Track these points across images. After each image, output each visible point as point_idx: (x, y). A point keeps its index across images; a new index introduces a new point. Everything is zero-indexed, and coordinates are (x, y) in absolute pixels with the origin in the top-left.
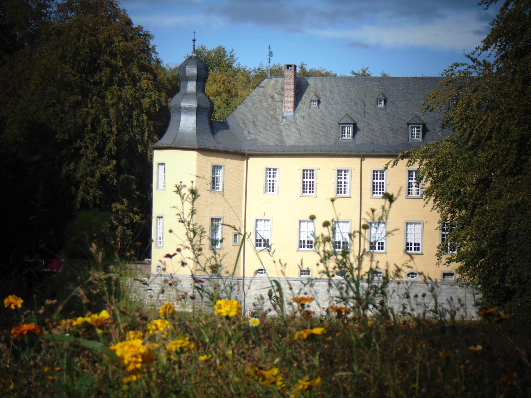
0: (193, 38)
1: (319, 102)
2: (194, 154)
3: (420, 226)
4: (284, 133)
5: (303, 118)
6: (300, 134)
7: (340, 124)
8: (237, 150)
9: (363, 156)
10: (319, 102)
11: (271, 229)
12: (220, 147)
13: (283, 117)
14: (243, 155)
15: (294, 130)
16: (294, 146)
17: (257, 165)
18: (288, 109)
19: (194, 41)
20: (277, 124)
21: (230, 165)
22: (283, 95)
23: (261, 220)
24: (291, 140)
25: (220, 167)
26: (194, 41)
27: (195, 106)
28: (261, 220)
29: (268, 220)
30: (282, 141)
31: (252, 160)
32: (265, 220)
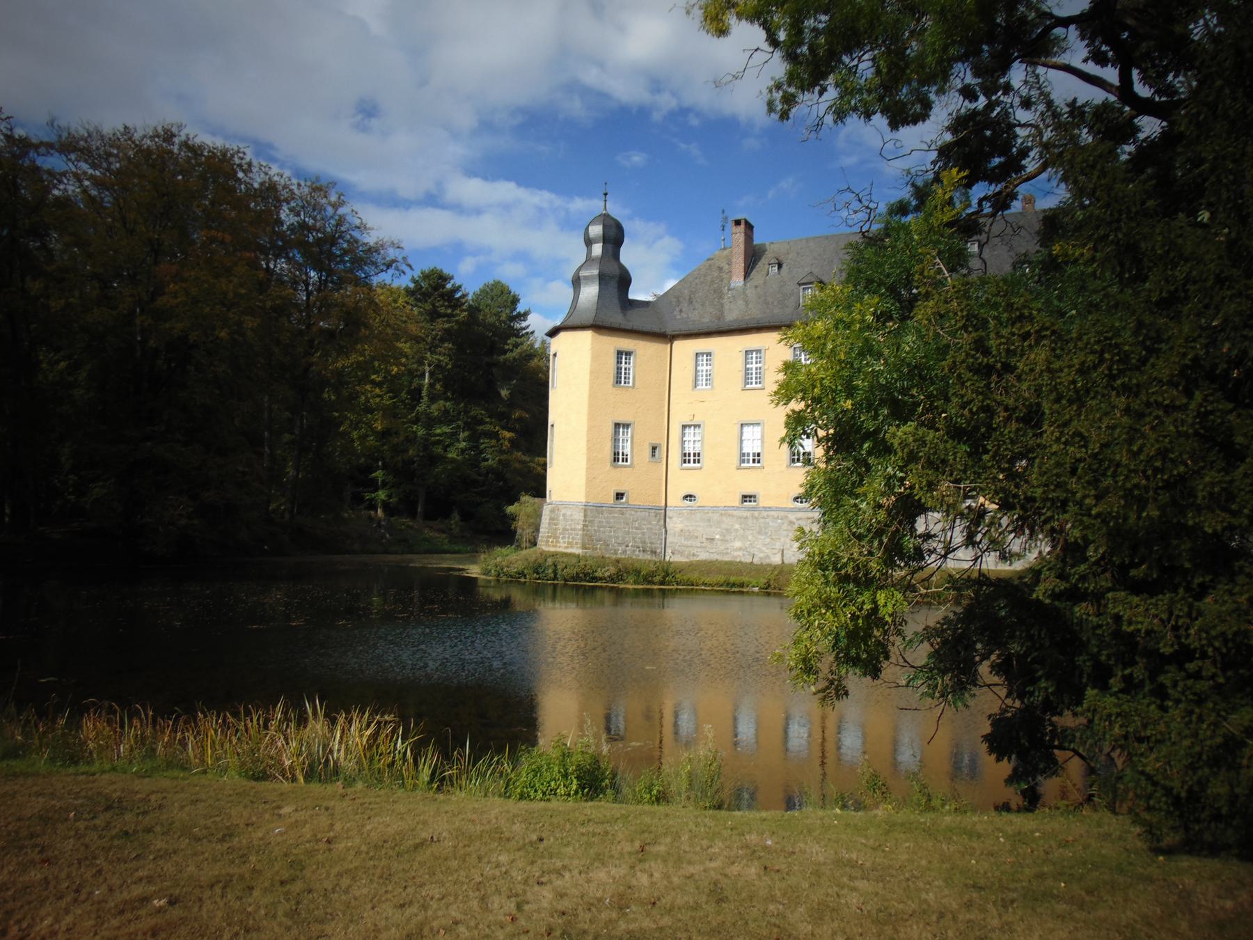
1: (780, 266)
2: (588, 335)
4: (726, 307)
7: (800, 285)
8: (656, 329)
10: (780, 266)
11: (703, 437)
12: (629, 326)
14: (667, 337)
15: (740, 302)
17: (685, 349)
18: (738, 281)
20: (721, 297)
21: (645, 350)
23: (690, 426)
24: (733, 314)
25: (629, 354)
27: (596, 272)
28: (690, 426)
30: (720, 317)
31: (678, 344)
32: (695, 426)
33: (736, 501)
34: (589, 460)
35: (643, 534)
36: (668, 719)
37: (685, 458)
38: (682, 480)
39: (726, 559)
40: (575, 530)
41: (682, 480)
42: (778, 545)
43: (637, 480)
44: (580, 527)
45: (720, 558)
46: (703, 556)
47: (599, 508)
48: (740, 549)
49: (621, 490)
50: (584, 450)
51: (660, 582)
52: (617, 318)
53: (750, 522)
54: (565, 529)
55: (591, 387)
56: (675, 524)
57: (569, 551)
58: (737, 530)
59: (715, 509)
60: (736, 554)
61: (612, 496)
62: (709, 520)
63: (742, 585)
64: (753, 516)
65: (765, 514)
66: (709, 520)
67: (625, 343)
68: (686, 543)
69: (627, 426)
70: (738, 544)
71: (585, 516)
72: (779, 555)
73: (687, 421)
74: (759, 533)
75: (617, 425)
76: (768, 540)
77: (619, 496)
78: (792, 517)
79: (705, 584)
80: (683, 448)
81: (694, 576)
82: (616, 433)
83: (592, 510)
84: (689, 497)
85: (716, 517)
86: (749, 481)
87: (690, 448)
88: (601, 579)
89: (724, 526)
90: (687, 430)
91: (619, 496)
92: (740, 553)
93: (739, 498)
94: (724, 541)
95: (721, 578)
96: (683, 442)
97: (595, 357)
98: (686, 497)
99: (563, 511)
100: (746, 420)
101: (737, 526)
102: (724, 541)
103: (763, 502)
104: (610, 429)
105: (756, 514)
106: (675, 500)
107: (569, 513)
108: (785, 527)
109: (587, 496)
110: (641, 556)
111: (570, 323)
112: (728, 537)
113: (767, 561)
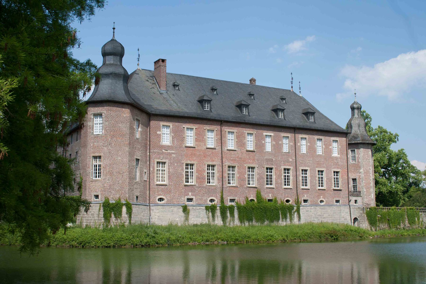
0: (113, 27)
5: (173, 95)
6: (177, 104)
19: (114, 29)
22: (154, 81)
26: (114, 29)
62: (172, 211)
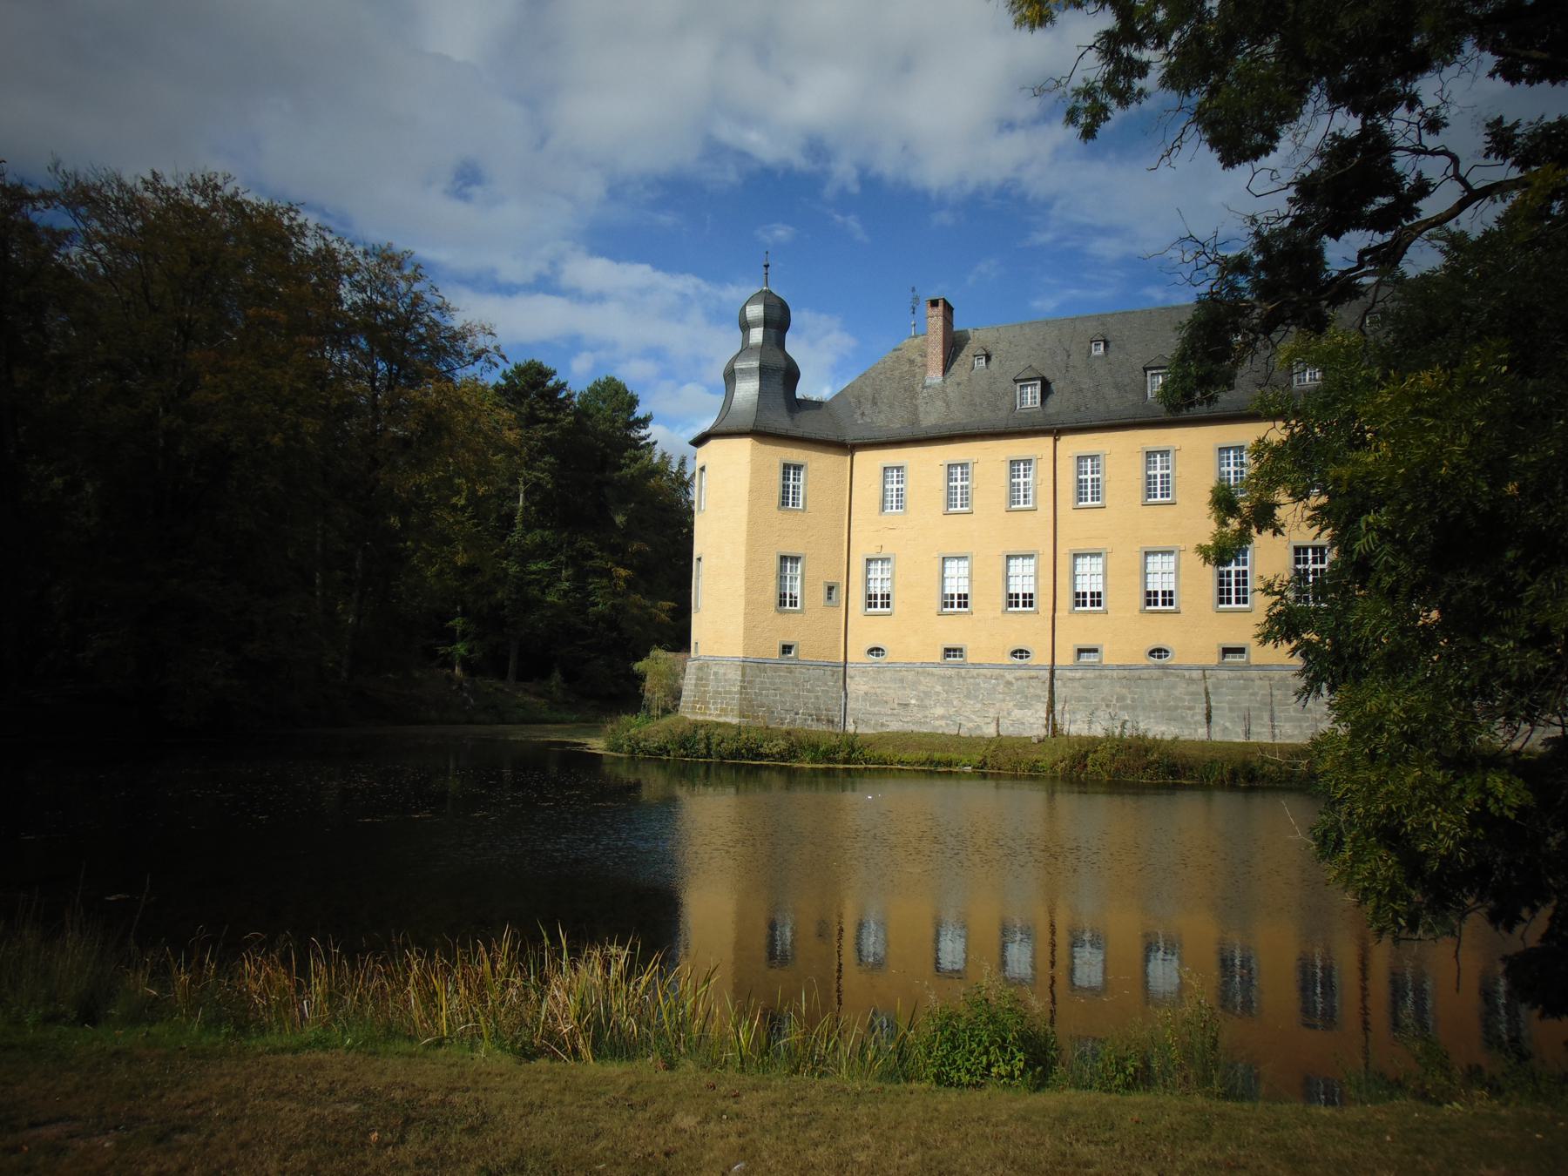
1: (988, 358)
2: (746, 444)
3: (1172, 558)
7: (1016, 381)
8: (832, 437)
9: (1056, 432)
10: (988, 358)
11: (893, 574)
12: (798, 432)
13: (924, 387)
14: (847, 447)
15: (939, 403)
16: (935, 426)
17: (869, 463)
18: (935, 376)
20: (914, 397)
21: (819, 465)
23: (876, 560)
24: (931, 418)
25: (798, 468)
27: (756, 364)
28: (876, 560)
29: (888, 560)
30: (915, 422)
31: (860, 456)
32: (883, 560)
33: (938, 657)
34: (748, 603)
35: (817, 698)
36: (850, 932)
37: (871, 601)
38: (866, 629)
39: (925, 730)
40: (730, 692)
41: (866, 629)
42: (992, 713)
43: (809, 630)
44: (736, 689)
45: (916, 729)
46: (894, 726)
47: (760, 664)
48: (942, 717)
49: (788, 641)
50: (742, 591)
51: (843, 761)
52: (782, 422)
53: (955, 682)
54: (717, 692)
55: (750, 512)
56: (857, 686)
57: (721, 720)
58: (938, 693)
59: (909, 666)
60: (937, 723)
61: (778, 648)
63: (949, 764)
64: (959, 676)
65: (975, 672)
66: (902, 681)
67: (794, 454)
68: (874, 709)
69: (795, 559)
70: (939, 711)
71: (743, 675)
72: (993, 726)
73: (872, 554)
74: (968, 696)
75: (784, 559)
76: (979, 706)
77: (786, 649)
78: (1009, 676)
79: (902, 763)
80: (868, 588)
81: (888, 752)
82: (782, 568)
83: (751, 667)
84: (875, 651)
85: (910, 676)
86: (954, 630)
87: (877, 588)
88: (767, 756)
89: (922, 688)
90: (872, 566)
91: (786, 649)
92: (943, 723)
93: (940, 651)
94: (922, 707)
95: (923, 755)
96: (868, 581)
97: (756, 471)
98: (871, 651)
99: (715, 669)
100: (948, 552)
101: (939, 688)
102: (922, 707)
103: (971, 657)
104: (775, 562)
105: (963, 672)
106: (857, 655)
107: (722, 671)
108: (1001, 688)
109: (746, 646)
110: (815, 727)
111: (723, 428)
112: (927, 702)
113: (978, 733)
